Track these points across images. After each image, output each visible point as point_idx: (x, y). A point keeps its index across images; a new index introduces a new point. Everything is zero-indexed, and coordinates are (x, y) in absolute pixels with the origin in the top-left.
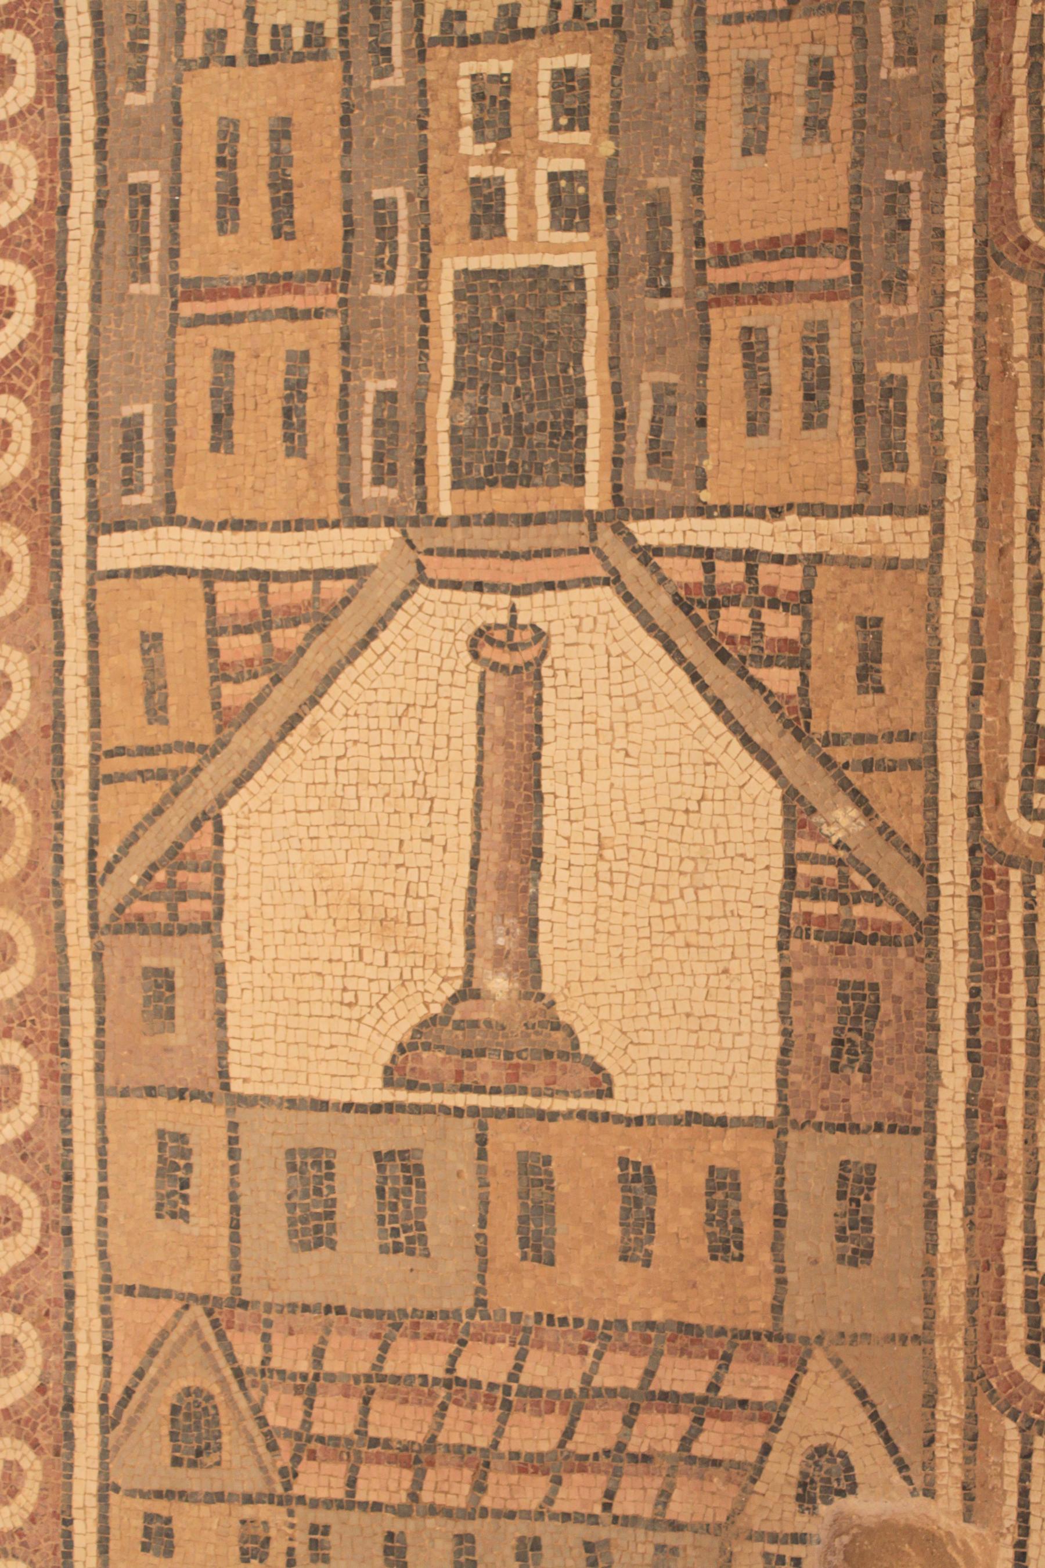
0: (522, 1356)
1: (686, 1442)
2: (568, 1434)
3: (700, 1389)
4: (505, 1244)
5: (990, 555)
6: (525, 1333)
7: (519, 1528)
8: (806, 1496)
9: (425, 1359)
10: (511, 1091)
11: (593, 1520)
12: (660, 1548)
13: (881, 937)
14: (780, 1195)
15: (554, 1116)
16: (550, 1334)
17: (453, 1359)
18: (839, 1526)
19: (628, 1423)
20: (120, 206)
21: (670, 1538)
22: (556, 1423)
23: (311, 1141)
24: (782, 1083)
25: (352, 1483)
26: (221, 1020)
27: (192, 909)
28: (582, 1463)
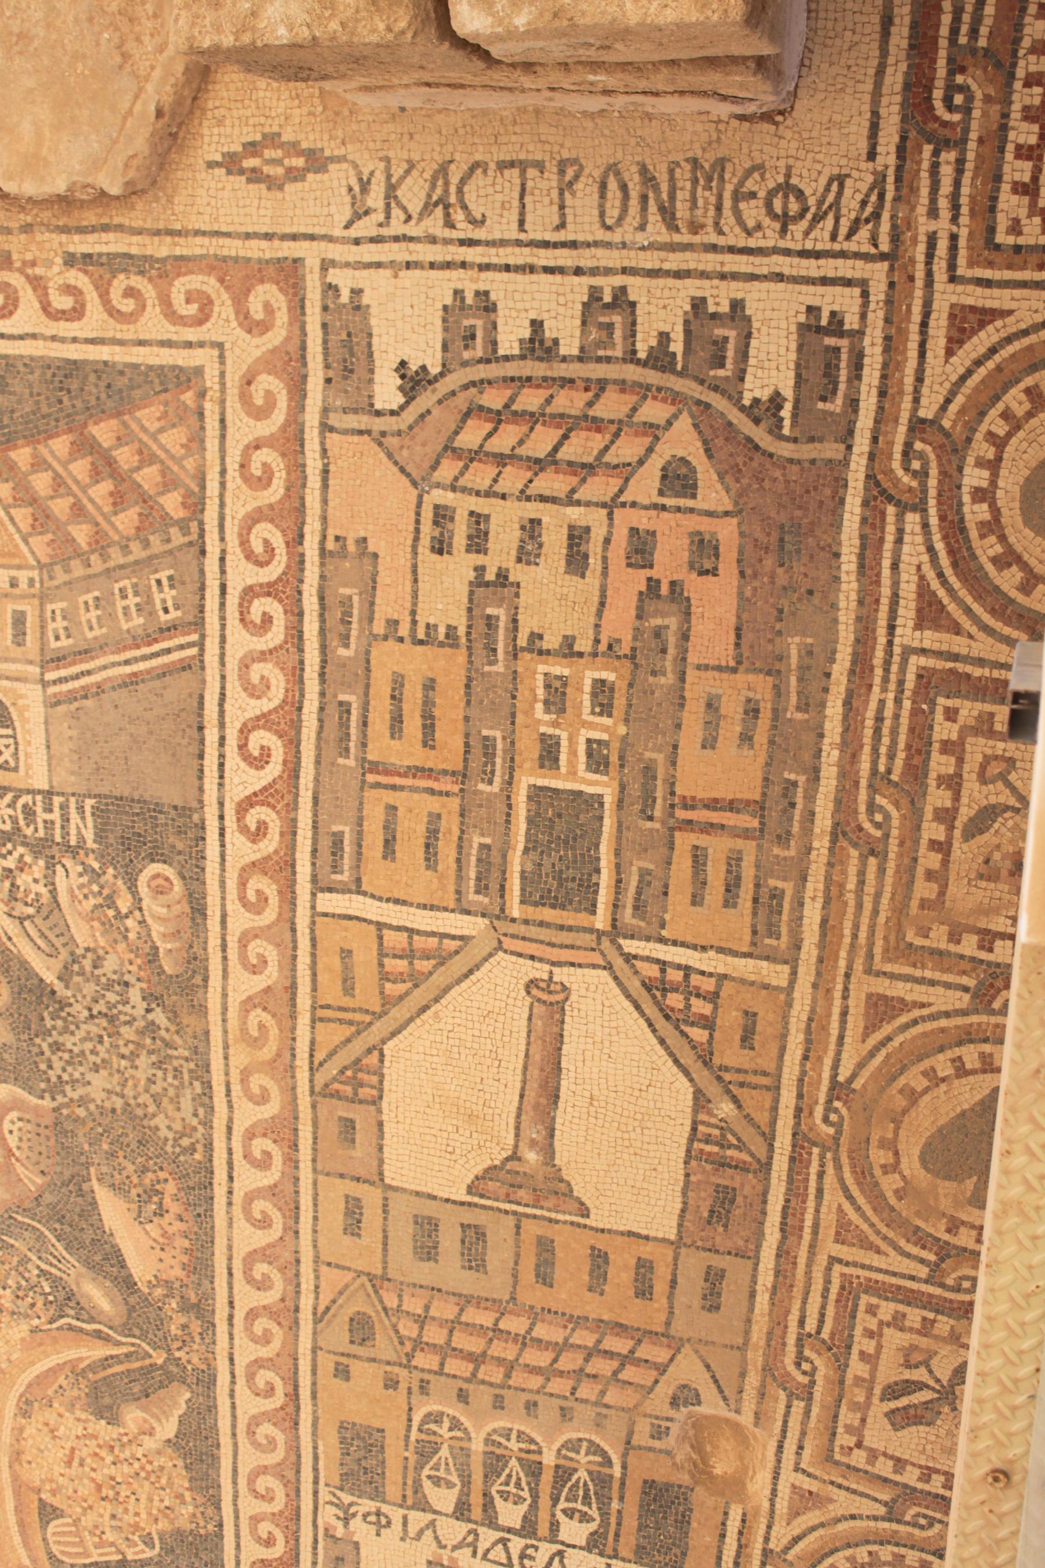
1: (615, 1373)
4: (528, 1275)
5: (821, 993)
6: (535, 1315)
7: (525, 1397)
8: (674, 1402)
13: (740, 1167)
16: (549, 1317)
19: (587, 1360)
20: (332, 711)
23: (426, 1213)
24: (680, 1225)
26: (381, 1148)
27: (365, 1092)
28: (561, 1374)
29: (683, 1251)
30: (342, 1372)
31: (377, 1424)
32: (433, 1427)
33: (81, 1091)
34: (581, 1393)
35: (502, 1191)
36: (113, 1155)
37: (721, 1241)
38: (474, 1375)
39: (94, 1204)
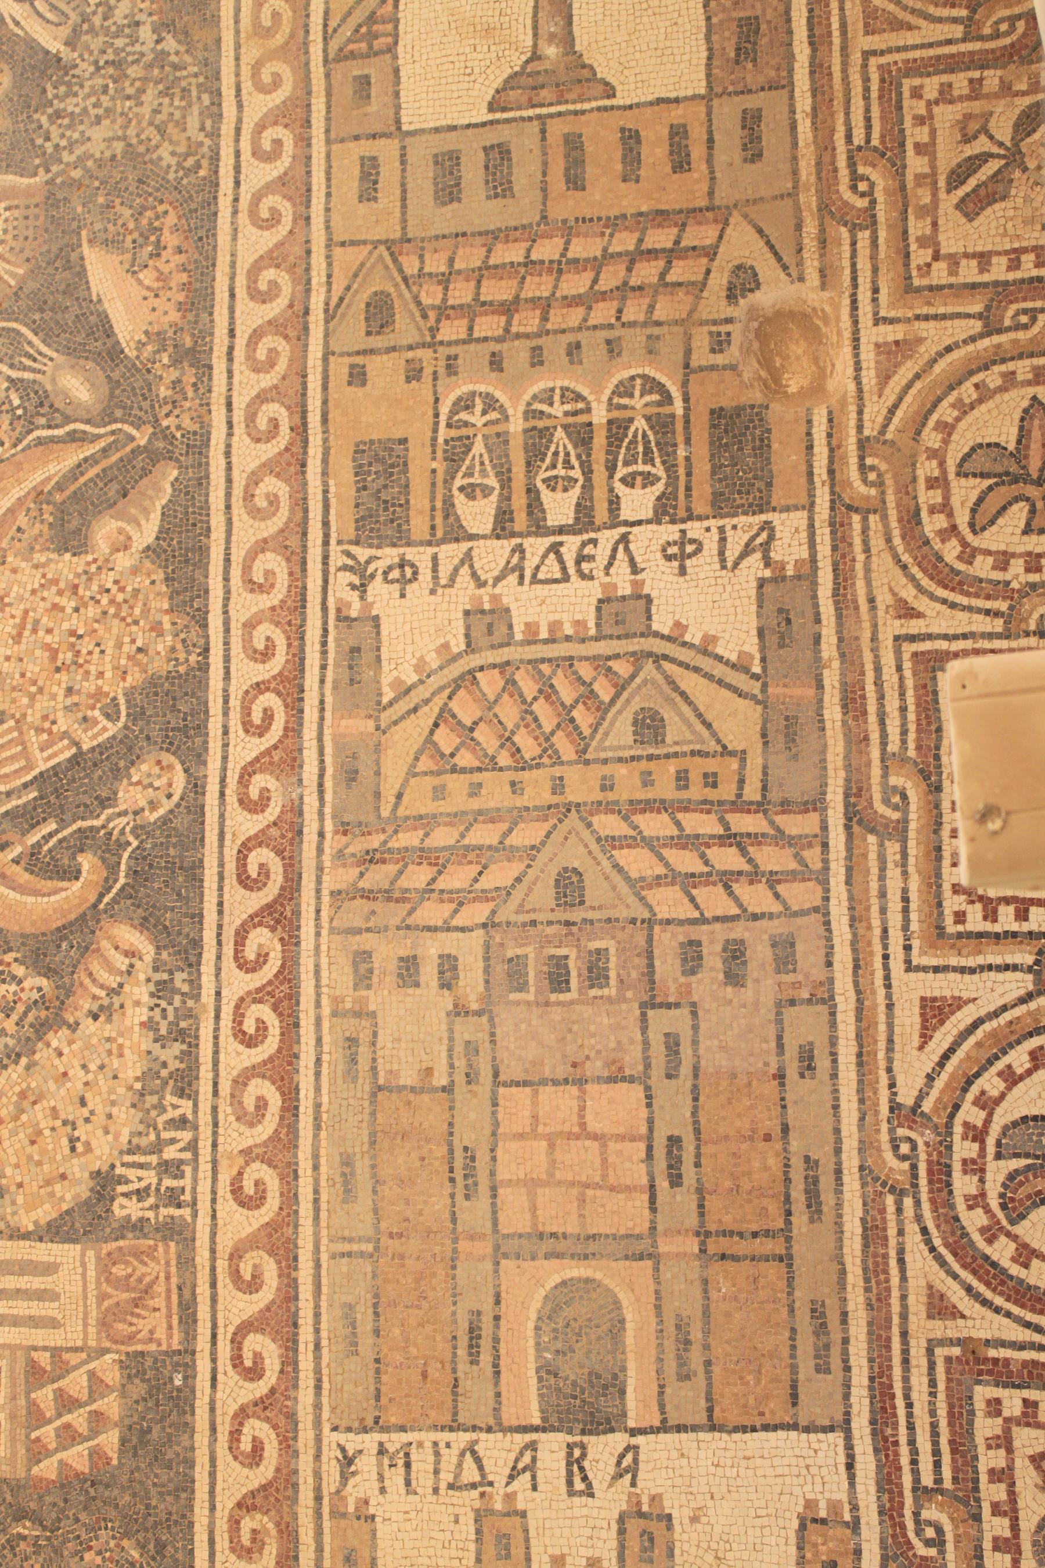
0: (568, 243)
1: (662, 276)
2: (595, 281)
3: (669, 245)
7: (569, 338)
9: (512, 253)
10: (559, 103)
11: (611, 326)
12: (649, 337)
14: (710, 133)
15: (583, 112)
16: (583, 228)
17: (529, 250)
18: (753, 312)
19: (629, 270)
21: (656, 331)
22: (588, 276)
24: (709, 76)
25: (471, 329)
28: (603, 296)
29: (716, 102)
30: (358, 376)
31: (399, 435)
32: (464, 416)
33: (79, 151)
34: (628, 316)
35: (524, 99)
36: (110, 206)
37: (753, 79)
38: (507, 330)
39: (82, 273)
